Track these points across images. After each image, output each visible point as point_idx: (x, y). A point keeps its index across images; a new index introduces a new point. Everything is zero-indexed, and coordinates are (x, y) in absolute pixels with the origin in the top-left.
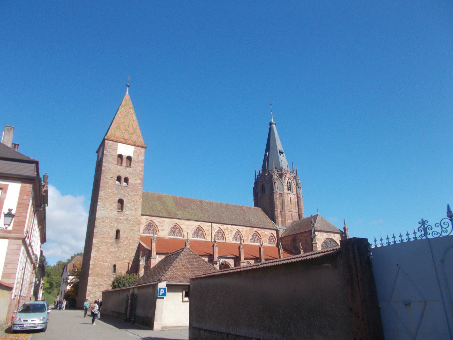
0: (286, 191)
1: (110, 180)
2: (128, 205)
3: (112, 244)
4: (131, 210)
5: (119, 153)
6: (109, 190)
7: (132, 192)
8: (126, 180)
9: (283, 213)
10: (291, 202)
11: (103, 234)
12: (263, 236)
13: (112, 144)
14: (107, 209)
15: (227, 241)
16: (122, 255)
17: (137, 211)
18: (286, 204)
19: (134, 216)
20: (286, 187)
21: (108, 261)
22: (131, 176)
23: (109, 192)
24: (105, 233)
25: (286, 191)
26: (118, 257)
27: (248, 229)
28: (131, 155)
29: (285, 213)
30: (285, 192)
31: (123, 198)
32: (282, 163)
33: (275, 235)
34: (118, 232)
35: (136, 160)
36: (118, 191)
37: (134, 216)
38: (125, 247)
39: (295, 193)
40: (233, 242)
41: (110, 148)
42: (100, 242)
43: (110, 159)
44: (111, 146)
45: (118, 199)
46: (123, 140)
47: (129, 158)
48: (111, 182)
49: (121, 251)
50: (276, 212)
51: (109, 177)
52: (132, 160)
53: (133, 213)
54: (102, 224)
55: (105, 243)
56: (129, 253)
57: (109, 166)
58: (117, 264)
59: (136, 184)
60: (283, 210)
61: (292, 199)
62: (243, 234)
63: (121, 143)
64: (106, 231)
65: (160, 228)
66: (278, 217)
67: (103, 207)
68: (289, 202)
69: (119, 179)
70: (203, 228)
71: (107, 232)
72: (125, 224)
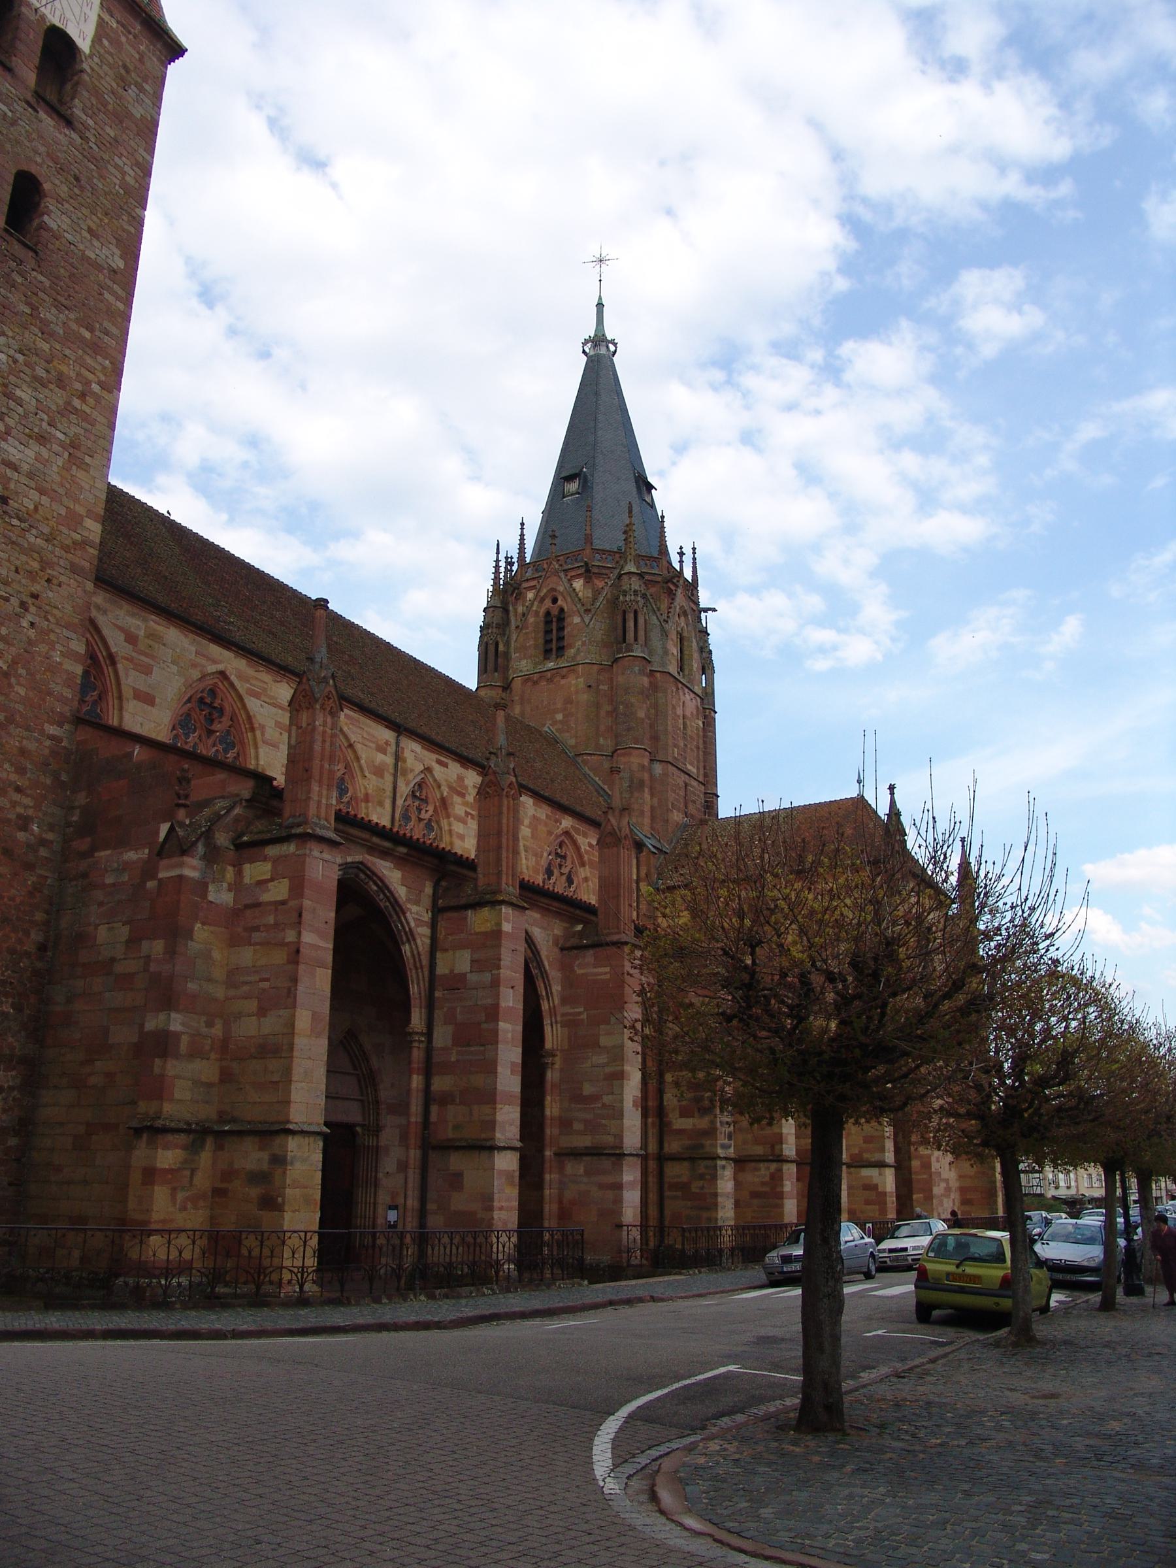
4: (42, 439)
22: (63, 190)
53: (54, 472)
65: (131, 679)
70: (358, 747)
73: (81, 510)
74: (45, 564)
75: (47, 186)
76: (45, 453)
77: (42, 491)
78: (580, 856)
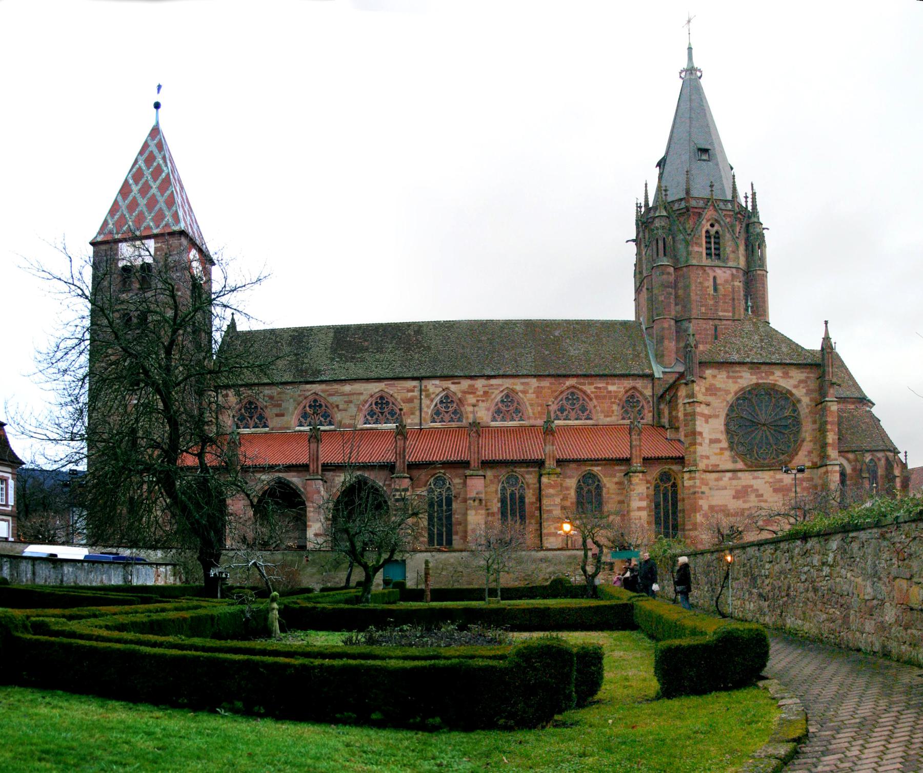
10: (716, 290)
12: (597, 397)
27: (546, 383)
40: (493, 424)
61: (718, 282)
68: (711, 291)
78: (588, 396)
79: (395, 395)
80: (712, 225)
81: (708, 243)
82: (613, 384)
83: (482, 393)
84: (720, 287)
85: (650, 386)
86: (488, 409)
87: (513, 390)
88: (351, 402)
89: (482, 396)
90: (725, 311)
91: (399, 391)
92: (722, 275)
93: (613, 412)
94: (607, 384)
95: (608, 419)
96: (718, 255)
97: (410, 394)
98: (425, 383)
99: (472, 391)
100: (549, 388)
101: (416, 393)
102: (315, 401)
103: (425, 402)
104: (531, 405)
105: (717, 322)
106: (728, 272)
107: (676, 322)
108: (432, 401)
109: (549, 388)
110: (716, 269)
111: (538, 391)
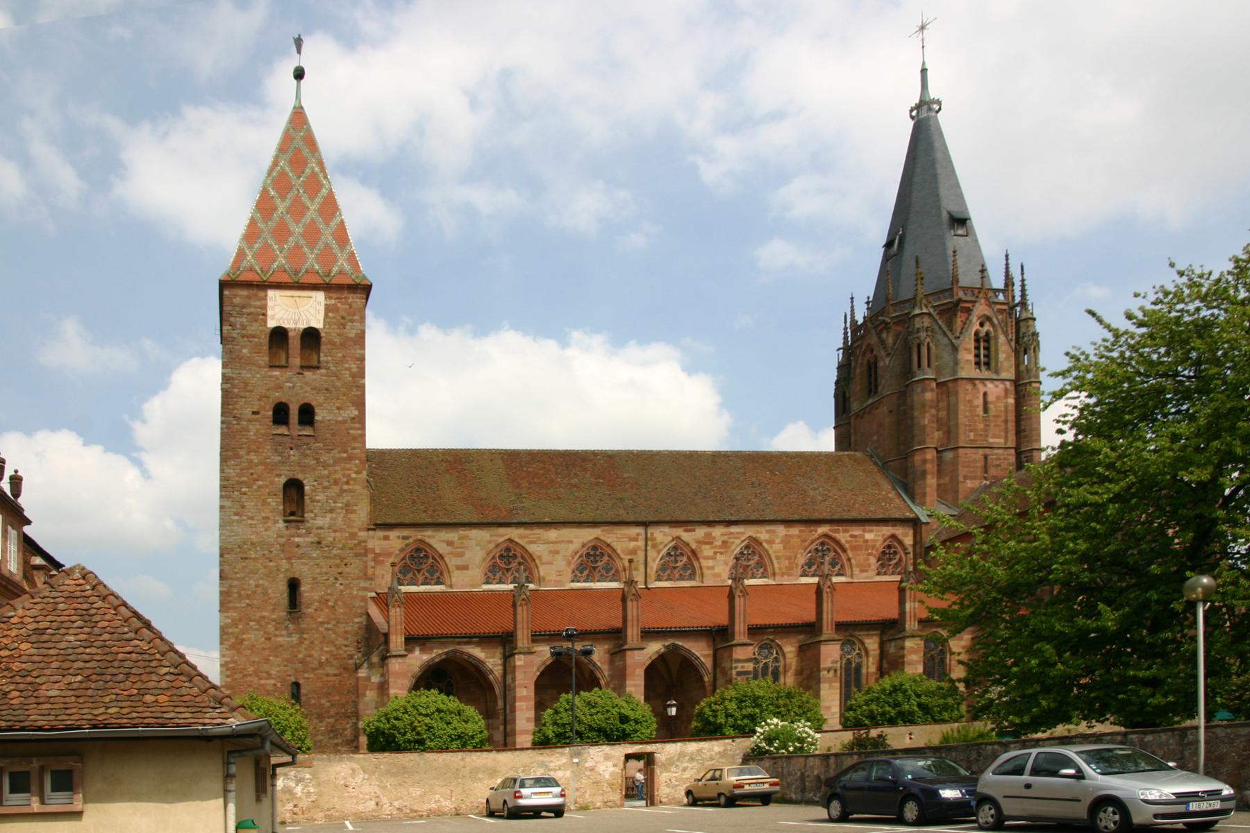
0: (968, 369)
1: (249, 421)
2: (320, 497)
3: (278, 624)
4: (331, 511)
5: (272, 324)
6: (253, 457)
7: (329, 451)
8: (307, 414)
9: (949, 455)
10: (986, 410)
11: (248, 597)
12: (854, 548)
13: (248, 297)
14: (252, 518)
15: (709, 582)
16: (315, 654)
17: (354, 512)
18: (962, 419)
19: (341, 530)
20: (967, 356)
21: (273, 672)
22: (321, 399)
23: (250, 461)
24: (254, 592)
25: (968, 369)
26: (302, 662)
27: (795, 531)
28: (318, 323)
29: (957, 457)
30: (963, 374)
31: (300, 477)
32: (960, 263)
33: (908, 541)
34: (294, 585)
35: (337, 340)
36: (281, 454)
37: (341, 530)
38: (321, 629)
39: (1009, 374)
41: (241, 314)
42: (240, 620)
43: (245, 351)
44: (244, 307)
45: (283, 480)
46: (284, 278)
47: (311, 337)
48: (253, 428)
49: (312, 643)
50: (918, 458)
51: (247, 412)
52: (323, 340)
54: (239, 566)
55: (258, 622)
56: (338, 648)
57: (246, 374)
58: (301, 681)
59: (345, 422)
60: (949, 444)
61: (991, 398)
62: (775, 549)
63: (279, 286)
64: (257, 586)
66: (924, 474)
67: (236, 514)
68: (980, 411)
69: (280, 414)
71: (259, 590)
72: (313, 559)
73: (356, 530)
74: (342, 559)
75: (313, 404)
76: (334, 515)
77: (335, 531)
79: (614, 545)
80: (982, 325)
81: (977, 348)
82: (871, 531)
83: (719, 543)
84: (991, 406)
85: (911, 532)
86: (726, 564)
87: (756, 540)
88: (557, 552)
89: (720, 547)
90: (995, 437)
91: (623, 540)
92: (995, 390)
93: (869, 565)
94: (864, 531)
95: (864, 574)
96: (987, 364)
97: (632, 544)
98: (651, 530)
99: (708, 541)
100: (799, 536)
101: (641, 543)
102: (508, 549)
103: (652, 554)
104: (778, 558)
105: (987, 451)
106: (1001, 386)
107: (938, 452)
108: (659, 552)
109: (799, 536)
110: (988, 383)
111: (786, 541)
